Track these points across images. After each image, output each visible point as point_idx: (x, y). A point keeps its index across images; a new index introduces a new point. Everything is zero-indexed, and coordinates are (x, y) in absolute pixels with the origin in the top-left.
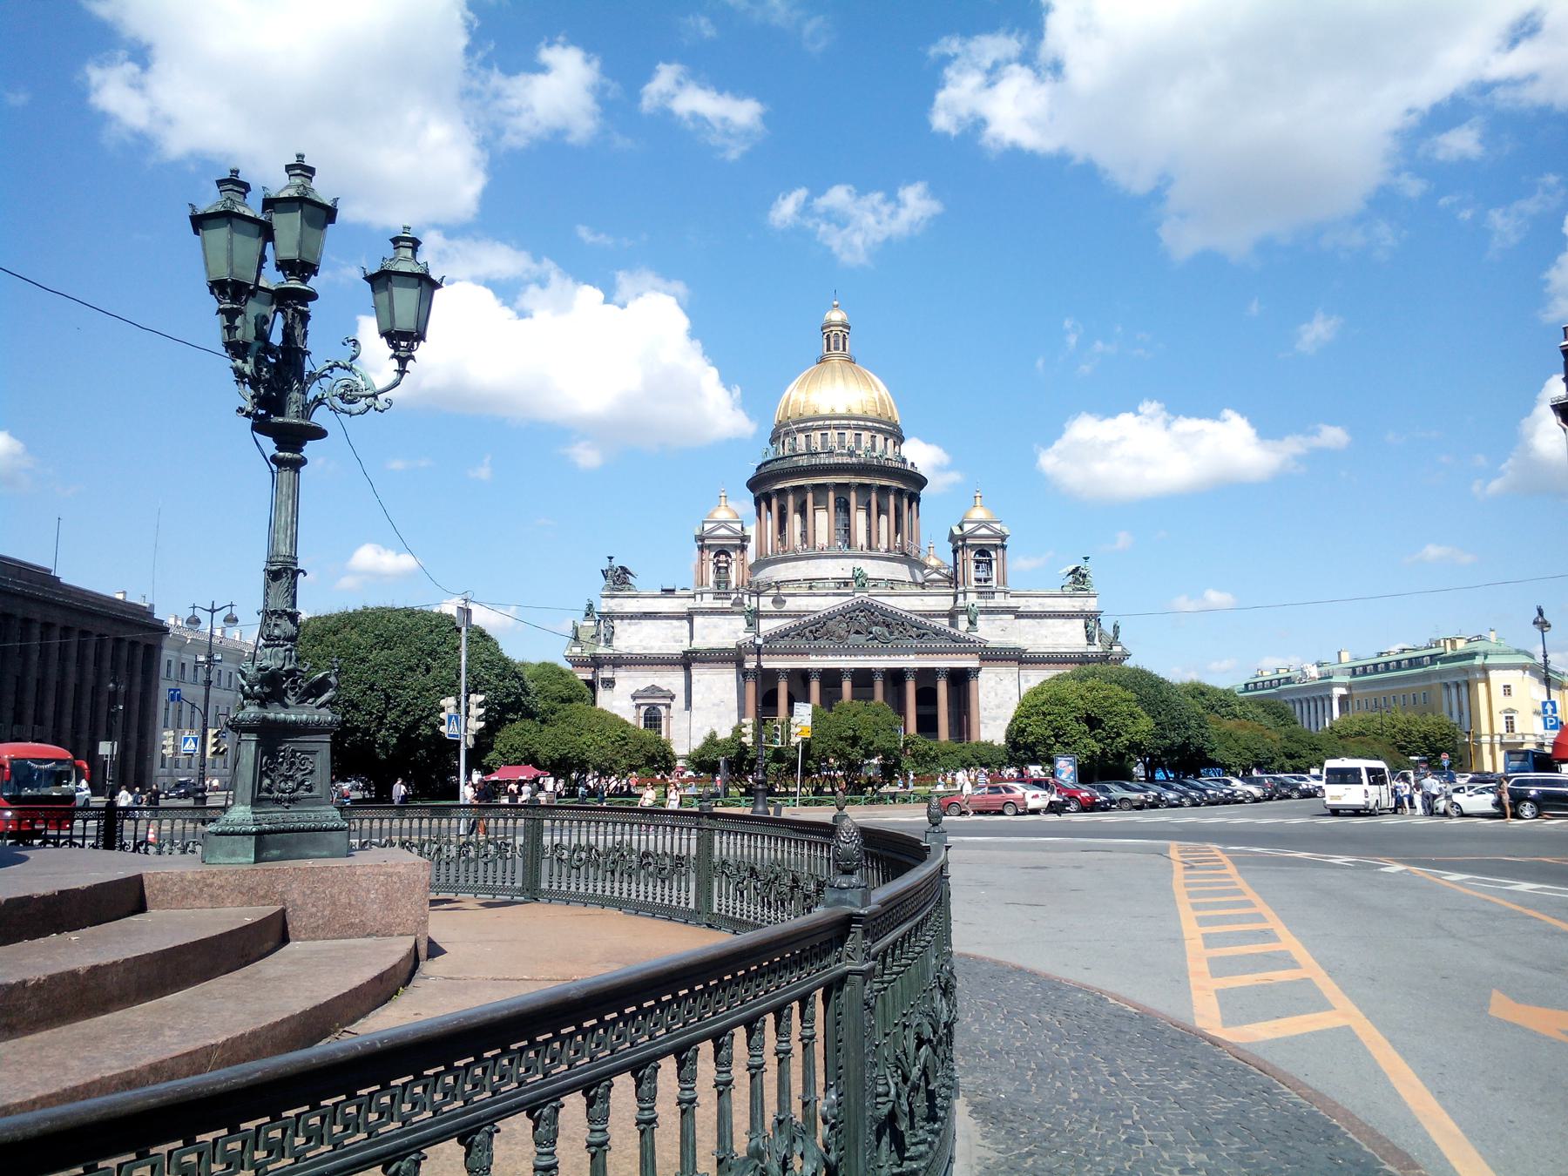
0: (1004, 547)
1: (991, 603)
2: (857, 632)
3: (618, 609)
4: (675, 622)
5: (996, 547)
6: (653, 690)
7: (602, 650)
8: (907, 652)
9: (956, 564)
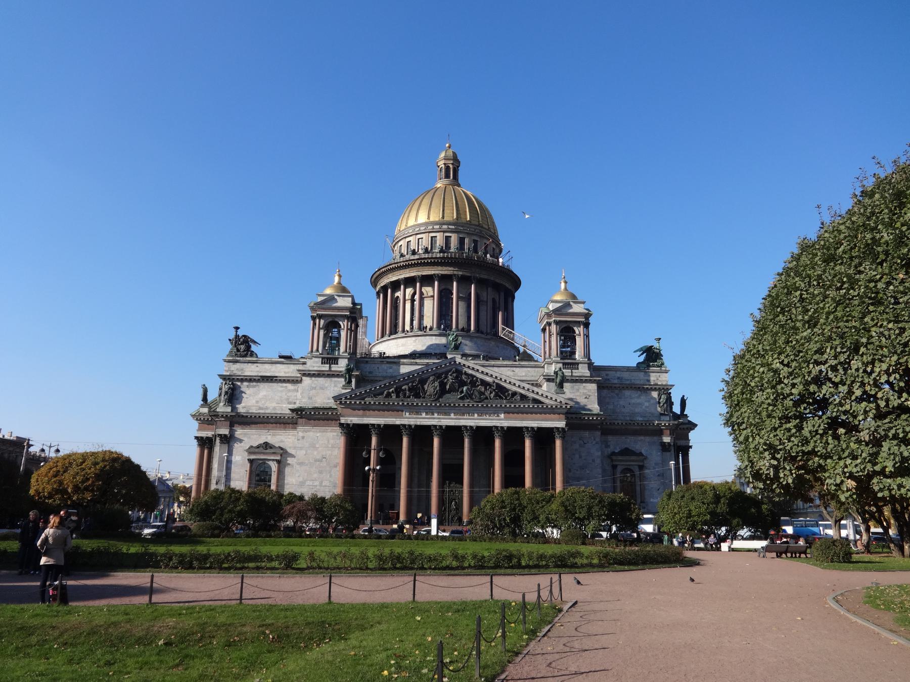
0: (587, 325)
1: (576, 373)
2: (449, 392)
3: (239, 373)
4: (290, 386)
5: (578, 323)
6: (266, 446)
7: (223, 408)
8: (496, 411)
9: (545, 342)
